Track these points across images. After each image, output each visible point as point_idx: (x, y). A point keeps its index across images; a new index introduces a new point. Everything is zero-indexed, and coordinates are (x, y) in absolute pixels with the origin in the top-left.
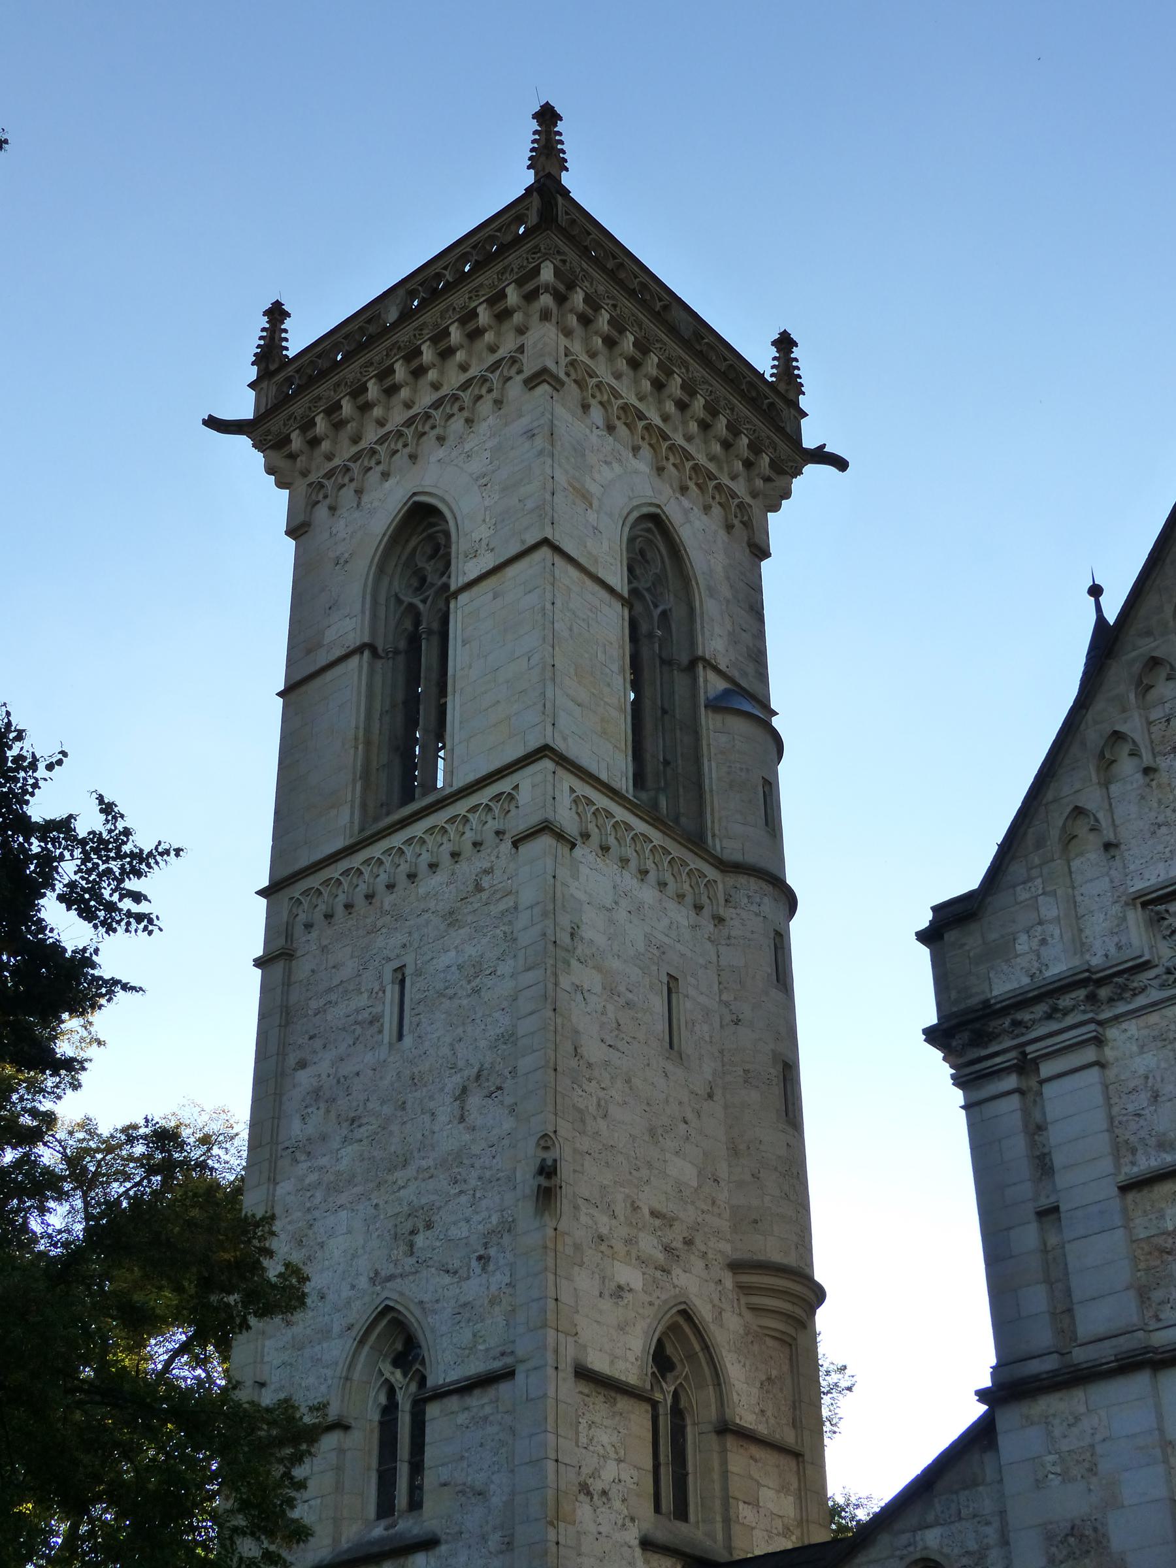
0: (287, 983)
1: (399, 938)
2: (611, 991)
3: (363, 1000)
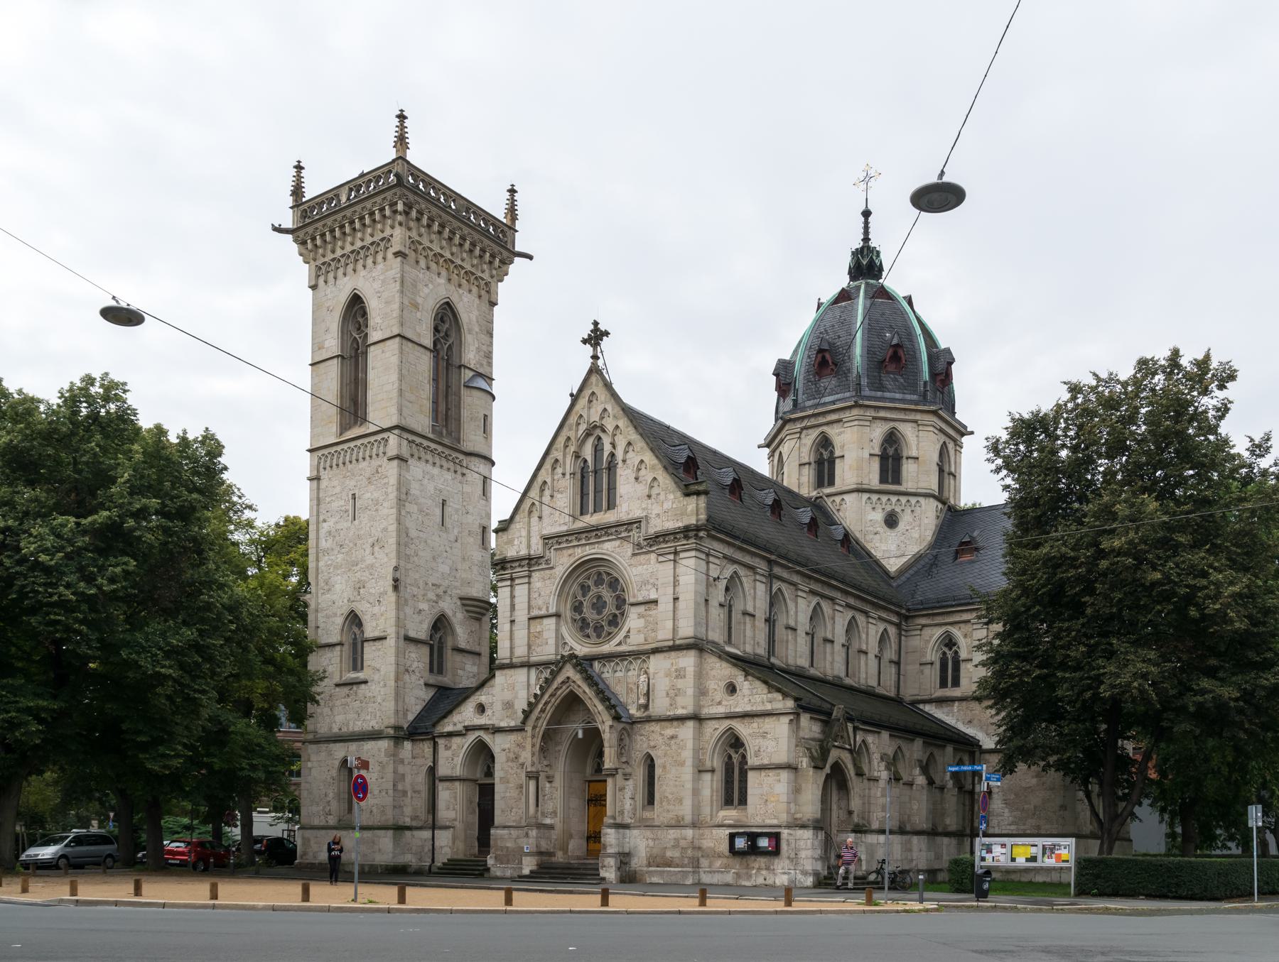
0: (318, 489)
1: (353, 483)
2: (421, 511)
3: (342, 503)
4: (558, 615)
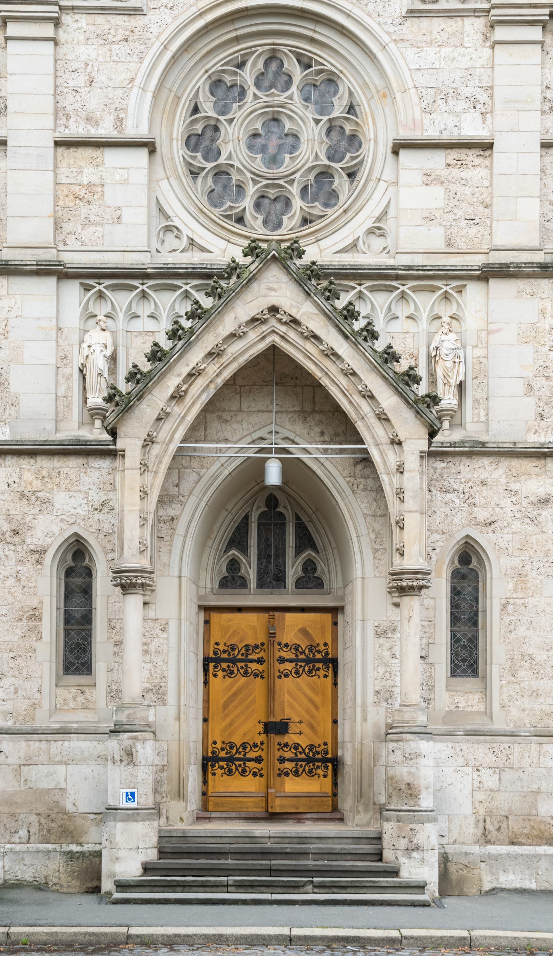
4: (150, 146)
